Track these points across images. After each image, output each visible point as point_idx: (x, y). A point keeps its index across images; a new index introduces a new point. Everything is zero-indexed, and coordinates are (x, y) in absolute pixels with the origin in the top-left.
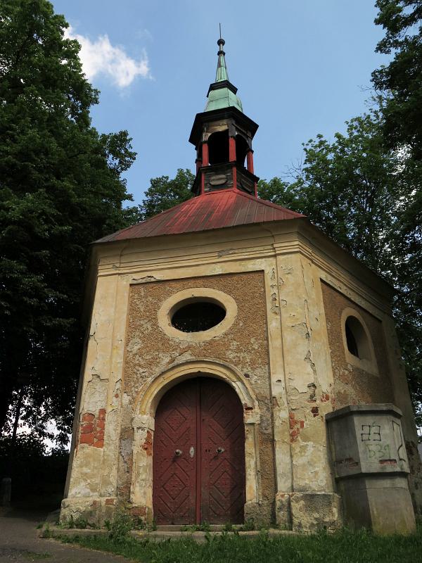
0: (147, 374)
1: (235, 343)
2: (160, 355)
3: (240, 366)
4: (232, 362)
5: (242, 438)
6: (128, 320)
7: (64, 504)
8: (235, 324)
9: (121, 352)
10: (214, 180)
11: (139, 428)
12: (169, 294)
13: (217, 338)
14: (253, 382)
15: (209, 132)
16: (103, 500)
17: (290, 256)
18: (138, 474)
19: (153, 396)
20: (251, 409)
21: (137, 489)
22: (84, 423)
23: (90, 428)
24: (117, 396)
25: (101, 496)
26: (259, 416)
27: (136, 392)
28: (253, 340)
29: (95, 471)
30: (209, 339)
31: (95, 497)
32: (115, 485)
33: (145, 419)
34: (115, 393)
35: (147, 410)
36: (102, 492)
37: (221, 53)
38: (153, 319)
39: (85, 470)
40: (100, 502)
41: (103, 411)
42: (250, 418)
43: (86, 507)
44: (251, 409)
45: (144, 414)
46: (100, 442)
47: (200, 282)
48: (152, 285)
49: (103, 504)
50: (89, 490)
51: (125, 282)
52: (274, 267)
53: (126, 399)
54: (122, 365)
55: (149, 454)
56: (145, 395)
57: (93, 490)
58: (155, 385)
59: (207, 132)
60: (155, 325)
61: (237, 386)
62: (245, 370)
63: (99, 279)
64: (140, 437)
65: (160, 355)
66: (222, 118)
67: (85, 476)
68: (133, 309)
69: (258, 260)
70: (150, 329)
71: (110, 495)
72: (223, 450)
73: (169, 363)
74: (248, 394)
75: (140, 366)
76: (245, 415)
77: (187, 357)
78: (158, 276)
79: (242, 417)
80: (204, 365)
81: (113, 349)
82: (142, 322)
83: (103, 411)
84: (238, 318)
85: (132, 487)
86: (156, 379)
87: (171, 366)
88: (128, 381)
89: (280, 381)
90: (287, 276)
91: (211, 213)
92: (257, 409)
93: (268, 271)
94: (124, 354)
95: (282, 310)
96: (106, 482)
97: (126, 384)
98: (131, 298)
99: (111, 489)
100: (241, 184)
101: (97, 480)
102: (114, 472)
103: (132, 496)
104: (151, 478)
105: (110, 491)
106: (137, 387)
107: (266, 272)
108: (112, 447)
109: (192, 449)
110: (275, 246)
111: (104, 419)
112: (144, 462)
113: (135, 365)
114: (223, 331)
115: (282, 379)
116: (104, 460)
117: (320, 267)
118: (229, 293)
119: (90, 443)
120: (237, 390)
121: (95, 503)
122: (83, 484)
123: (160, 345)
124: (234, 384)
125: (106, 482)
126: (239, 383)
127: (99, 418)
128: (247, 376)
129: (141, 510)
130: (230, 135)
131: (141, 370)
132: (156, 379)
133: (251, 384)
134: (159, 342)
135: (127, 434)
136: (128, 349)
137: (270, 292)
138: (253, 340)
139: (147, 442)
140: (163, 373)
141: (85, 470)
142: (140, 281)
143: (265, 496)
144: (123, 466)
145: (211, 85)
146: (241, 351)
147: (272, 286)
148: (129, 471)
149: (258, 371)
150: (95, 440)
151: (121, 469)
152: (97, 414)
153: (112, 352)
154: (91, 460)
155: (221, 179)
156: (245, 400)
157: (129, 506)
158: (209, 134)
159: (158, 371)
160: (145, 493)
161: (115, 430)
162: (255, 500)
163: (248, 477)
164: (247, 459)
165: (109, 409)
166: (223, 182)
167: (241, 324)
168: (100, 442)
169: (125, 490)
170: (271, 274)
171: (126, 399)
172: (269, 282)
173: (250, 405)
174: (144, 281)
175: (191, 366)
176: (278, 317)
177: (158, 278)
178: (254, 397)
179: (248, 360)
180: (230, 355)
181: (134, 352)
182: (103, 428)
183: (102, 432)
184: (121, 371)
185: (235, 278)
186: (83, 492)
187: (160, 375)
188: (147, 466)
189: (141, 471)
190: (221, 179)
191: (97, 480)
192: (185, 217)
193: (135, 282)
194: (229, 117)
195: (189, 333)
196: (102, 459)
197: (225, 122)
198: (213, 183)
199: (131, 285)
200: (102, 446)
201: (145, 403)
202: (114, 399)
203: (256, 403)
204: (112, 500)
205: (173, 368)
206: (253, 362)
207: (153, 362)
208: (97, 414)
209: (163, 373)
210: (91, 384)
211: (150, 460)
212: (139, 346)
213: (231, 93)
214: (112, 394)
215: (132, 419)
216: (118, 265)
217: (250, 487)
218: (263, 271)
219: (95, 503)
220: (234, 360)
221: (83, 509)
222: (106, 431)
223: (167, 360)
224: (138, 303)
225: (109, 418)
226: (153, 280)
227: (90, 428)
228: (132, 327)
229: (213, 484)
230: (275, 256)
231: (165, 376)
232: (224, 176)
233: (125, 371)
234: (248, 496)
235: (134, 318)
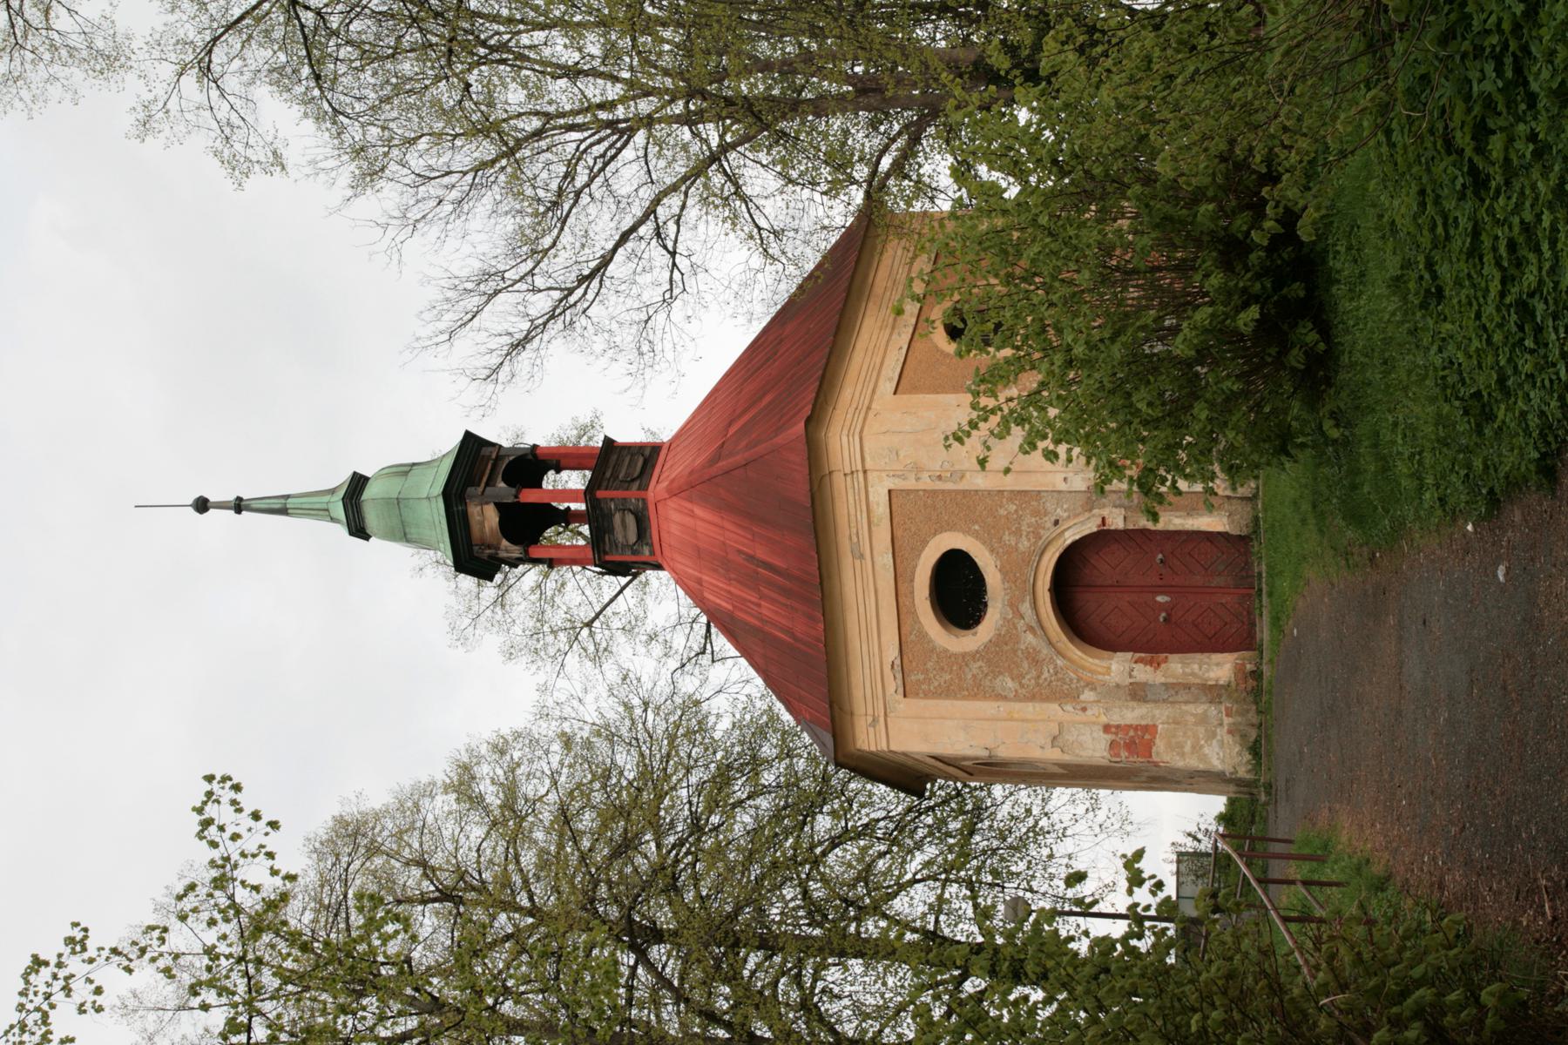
0: (1051, 667)
1: (1006, 537)
2: (1023, 647)
3: (1042, 532)
4: (1035, 543)
5: (1144, 532)
6: (964, 698)
7: (1231, 773)
8: (977, 536)
9: (1017, 706)
10: (625, 537)
11: (1131, 676)
12: (923, 635)
13: (998, 563)
14: (1065, 515)
15: (499, 543)
16: (1227, 721)
17: (866, 449)
18: (1193, 674)
19: (1084, 656)
20: (1103, 519)
21: (1212, 675)
22: (1124, 754)
23: (1130, 746)
24: (1084, 709)
25: (1221, 724)
26: (1114, 510)
27: (1078, 681)
28: (1002, 512)
29: (1190, 733)
30: (999, 576)
31: (1222, 732)
32: (1205, 707)
33: (1118, 667)
34: (1080, 713)
35: (1105, 664)
36: (1216, 723)
37: (239, 506)
38: (965, 658)
39: (1188, 748)
40: (1229, 725)
41: (1107, 728)
42: (1117, 522)
43: (1235, 742)
44: (1103, 519)
45: (1109, 668)
46: (1150, 729)
47: (902, 589)
48: (905, 661)
49: (1231, 720)
50: (1214, 742)
51: (903, 706)
52: (884, 474)
53: (1088, 695)
54: (1037, 705)
55: (1166, 660)
56: (1084, 668)
57: (1214, 735)
58: (1070, 654)
59: (497, 548)
60: (975, 656)
61: (1071, 537)
62: (1049, 524)
63: (893, 748)
64: (1143, 673)
65: (1023, 647)
66: (465, 516)
67: (1196, 748)
68: (947, 692)
69: (871, 498)
70: (980, 663)
71: (1220, 712)
72: (1160, 556)
73: (1034, 633)
74: (1082, 523)
75: (1039, 677)
76: (1113, 528)
77: (1026, 607)
78: (892, 653)
79: (1116, 531)
80: (1039, 583)
81: (1012, 719)
82: (969, 676)
83: (1107, 728)
84: (967, 532)
85: (1210, 683)
86: (1059, 653)
87: (1039, 632)
88: (1062, 693)
89: (1065, 479)
90: (901, 457)
91: (751, 558)
92: (1105, 512)
93: (891, 483)
94: (1020, 701)
95: (957, 467)
96: (1203, 720)
97: (1067, 696)
98: (927, 695)
99: (1213, 711)
100: (633, 480)
101: (1201, 730)
102: (1190, 708)
103: (1221, 682)
104: (1198, 656)
105: (1215, 713)
106: (1071, 680)
107: (892, 486)
108: (1157, 712)
109: (1160, 599)
110: (848, 471)
111: (1118, 727)
112: (1178, 667)
113: (1038, 685)
114: (987, 554)
115: (1063, 475)
116: (1174, 723)
117: (874, 391)
118: (925, 543)
119: (1149, 746)
120: (1077, 537)
121: (1230, 732)
122: (1206, 750)
123: (1006, 648)
124: (1069, 542)
125: (1203, 720)
126: (1067, 534)
127: (1116, 734)
128: (1056, 523)
129: (1239, 670)
130: (511, 500)
131: (1046, 675)
132: (1059, 653)
133: (1069, 517)
134: (1000, 654)
135: (1138, 693)
136: (1012, 695)
137: (926, 483)
138: (1002, 512)
139: (1150, 663)
140: (1050, 643)
141: (1188, 748)
142: (900, 682)
143: (1220, 507)
145: (351, 533)
146: (1019, 530)
147: (918, 479)
148: (1187, 687)
149: (1050, 506)
150: (1147, 737)
151: (1185, 698)
152: (1109, 737)
153: (1017, 720)
154: (1173, 741)
155: (623, 522)
156: (1091, 527)
157: (1233, 684)
158: (505, 543)
159: (1045, 651)
160: (1218, 664)
161: (1133, 709)
162: (1225, 520)
163: (1195, 528)
164: (1171, 528)
165: (1104, 719)
166: (631, 520)
167: (977, 527)
168: (1150, 729)
169: (1213, 692)
170: (897, 480)
171: (1088, 695)
172: (910, 484)
173: (1099, 521)
174: (899, 676)
175: (1040, 602)
176: (968, 474)
177: (896, 653)
178: (1087, 515)
179: (1033, 520)
180: (1024, 544)
181: (1017, 685)
182: (1130, 726)
183: (1136, 728)
184: (1045, 705)
185: (898, 533)
186: (1217, 750)
187: (1053, 646)
188: (1182, 662)
189: (1188, 670)
190: (623, 522)
191: (1201, 730)
192: (759, 605)
193: (901, 690)
194: (462, 499)
195: (989, 604)
196: (1173, 726)
197: (474, 510)
198: (632, 538)
199: (905, 696)
200: (1155, 726)
201: (1094, 667)
202: (1089, 712)
203: (1096, 511)
204: (1227, 709)
205: (1042, 628)
206: (1036, 513)
207: (1035, 660)
208: (1109, 737)
209: (1050, 643)
210: (1066, 749)
212: (1008, 680)
213: (369, 493)
214: (1080, 717)
215: (1118, 686)
216: (870, 719)
217: (1208, 525)
218: (890, 491)
219: (1230, 732)
220: (1033, 540)
221: (1237, 749)
222: (1135, 723)
223: (1030, 637)
224: (936, 684)
225: (1116, 718)
226: (898, 662)
227: (1130, 746)
228: (977, 691)
229: (1206, 569)
230: (865, 472)
231: (1054, 641)
232: (617, 518)
233: (1047, 699)
234: (1220, 529)
235: (961, 689)
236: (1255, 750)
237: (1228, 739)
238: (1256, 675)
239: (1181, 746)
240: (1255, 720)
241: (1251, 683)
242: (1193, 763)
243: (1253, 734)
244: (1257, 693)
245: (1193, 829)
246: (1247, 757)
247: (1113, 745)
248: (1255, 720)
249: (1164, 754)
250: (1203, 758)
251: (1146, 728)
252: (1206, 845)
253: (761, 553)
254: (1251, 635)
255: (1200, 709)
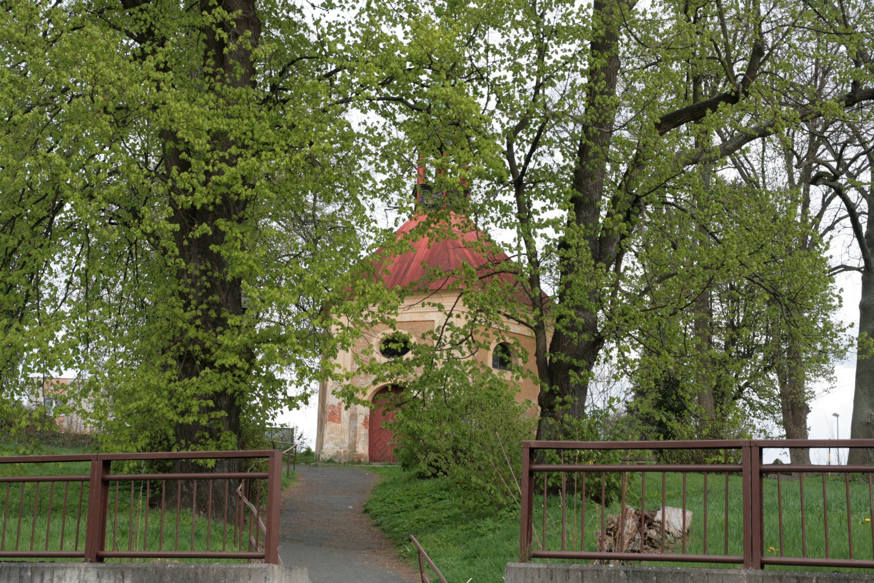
16: (342, 451)
22: (330, 411)
23: (333, 413)
31: (338, 449)
57: (337, 445)
64: (361, 419)
67: (332, 439)
91: (412, 260)
96: (343, 442)
99: (346, 445)
101: (339, 441)
102: (347, 436)
104: (367, 440)
119: (333, 420)
125: (343, 442)
129: (361, 456)
139: (365, 421)
144: (352, 434)
148: (355, 436)
152: (336, 405)
169: (353, 446)
183: (340, 416)
185: (418, 324)
191: (339, 441)
208: (336, 405)
211: (367, 431)
227: (333, 413)
236: (330, 461)
237: (335, 451)
238: (359, 462)
239: (333, 433)
240: (342, 461)
241: (356, 460)
242: (326, 437)
243: (337, 461)
244: (352, 462)
245: (304, 436)
246: (328, 458)
247: (334, 406)
248: (342, 461)
249: (330, 426)
250: (328, 442)
251: (339, 419)
252: (296, 441)
253: (414, 265)
254: (375, 461)
255: (347, 441)
